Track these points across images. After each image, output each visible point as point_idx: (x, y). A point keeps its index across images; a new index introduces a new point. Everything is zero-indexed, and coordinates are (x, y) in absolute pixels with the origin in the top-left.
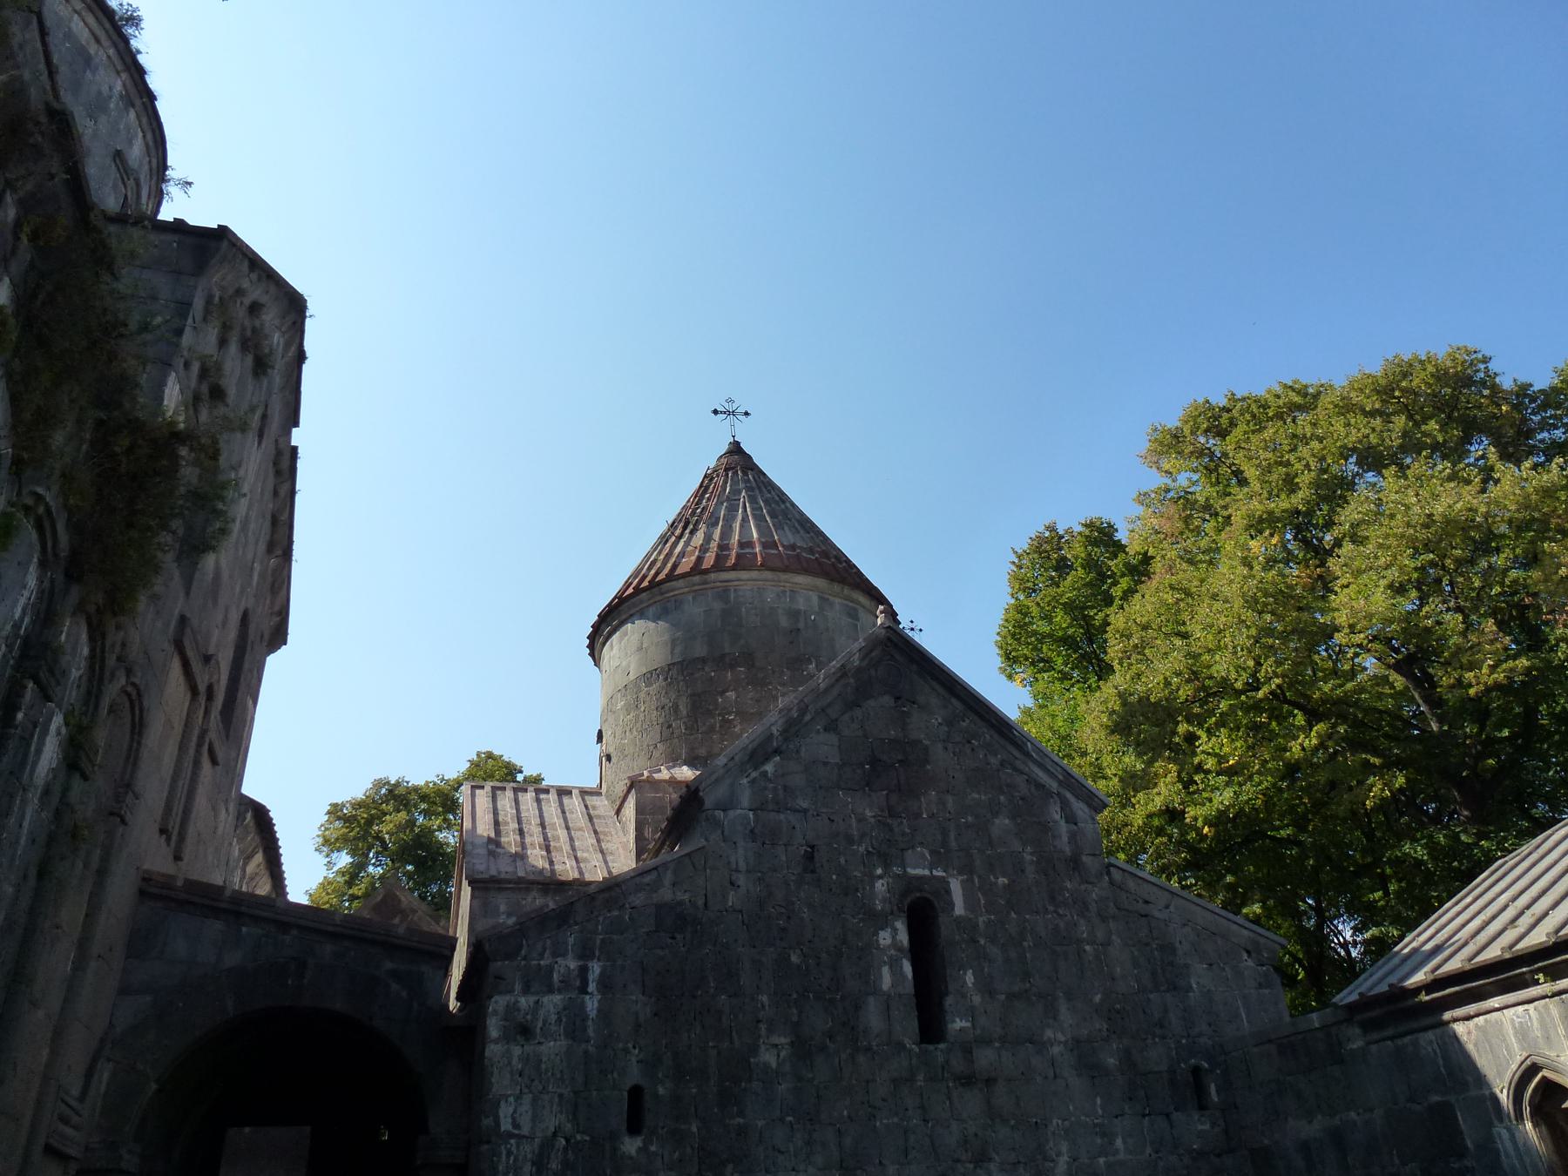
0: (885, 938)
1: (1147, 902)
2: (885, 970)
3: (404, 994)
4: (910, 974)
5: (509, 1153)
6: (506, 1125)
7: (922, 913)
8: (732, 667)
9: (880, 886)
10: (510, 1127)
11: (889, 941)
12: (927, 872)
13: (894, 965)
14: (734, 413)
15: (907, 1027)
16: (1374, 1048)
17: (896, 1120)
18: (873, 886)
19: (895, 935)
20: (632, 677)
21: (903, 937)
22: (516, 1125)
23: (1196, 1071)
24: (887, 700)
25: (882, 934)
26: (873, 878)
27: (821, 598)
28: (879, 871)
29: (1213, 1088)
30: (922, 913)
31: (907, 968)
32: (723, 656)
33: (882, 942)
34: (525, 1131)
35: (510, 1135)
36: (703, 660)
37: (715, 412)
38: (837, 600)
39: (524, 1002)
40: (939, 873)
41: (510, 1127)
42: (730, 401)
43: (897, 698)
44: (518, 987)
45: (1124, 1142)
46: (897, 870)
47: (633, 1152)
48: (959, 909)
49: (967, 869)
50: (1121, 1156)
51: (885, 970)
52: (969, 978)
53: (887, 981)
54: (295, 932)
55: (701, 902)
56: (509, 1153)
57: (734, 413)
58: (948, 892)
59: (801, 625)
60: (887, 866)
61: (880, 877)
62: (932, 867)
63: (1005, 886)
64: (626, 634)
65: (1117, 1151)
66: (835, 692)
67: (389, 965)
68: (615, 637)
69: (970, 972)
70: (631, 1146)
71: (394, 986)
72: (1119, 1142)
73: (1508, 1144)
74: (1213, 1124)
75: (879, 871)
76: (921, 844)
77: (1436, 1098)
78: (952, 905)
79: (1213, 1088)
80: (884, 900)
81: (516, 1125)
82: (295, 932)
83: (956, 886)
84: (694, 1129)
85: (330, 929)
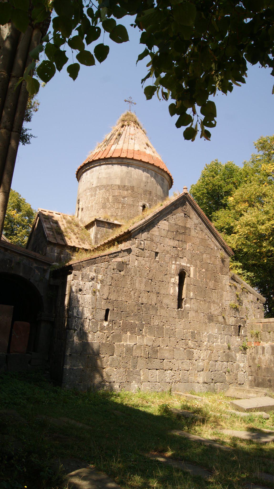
0: (173, 280)
2: (172, 288)
3: (39, 274)
4: (177, 291)
5: (76, 321)
6: (75, 314)
7: (182, 275)
8: (127, 190)
9: (173, 267)
10: (76, 315)
12: (185, 264)
13: (174, 288)
14: (131, 103)
15: (175, 304)
18: (172, 267)
19: (176, 279)
20: (94, 186)
21: (178, 281)
22: (78, 315)
24: (183, 214)
25: (172, 279)
27: (155, 173)
28: (174, 262)
29: (243, 331)
30: (182, 275)
32: (125, 186)
34: (80, 317)
35: (76, 317)
36: (119, 186)
37: (126, 101)
38: (159, 175)
39: (81, 283)
40: (188, 265)
41: (76, 315)
42: (131, 98)
43: (185, 214)
44: (80, 279)
45: (220, 341)
46: (177, 263)
48: (192, 276)
49: (196, 266)
50: (219, 344)
52: (192, 294)
53: (172, 291)
54: (9, 252)
56: (76, 321)
57: (131, 103)
59: (149, 181)
60: (176, 261)
62: (187, 263)
63: (204, 272)
64: (93, 172)
66: (169, 210)
67: (35, 265)
68: (88, 172)
69: (192, 293)
70: (105, 324)
71: (36, 271)
72: (219, 340)
74: (241, 340)
79: (243, 331)
81: (78, 315)
82: (9, 252)
83: (192, 269)
85: (19, 252)
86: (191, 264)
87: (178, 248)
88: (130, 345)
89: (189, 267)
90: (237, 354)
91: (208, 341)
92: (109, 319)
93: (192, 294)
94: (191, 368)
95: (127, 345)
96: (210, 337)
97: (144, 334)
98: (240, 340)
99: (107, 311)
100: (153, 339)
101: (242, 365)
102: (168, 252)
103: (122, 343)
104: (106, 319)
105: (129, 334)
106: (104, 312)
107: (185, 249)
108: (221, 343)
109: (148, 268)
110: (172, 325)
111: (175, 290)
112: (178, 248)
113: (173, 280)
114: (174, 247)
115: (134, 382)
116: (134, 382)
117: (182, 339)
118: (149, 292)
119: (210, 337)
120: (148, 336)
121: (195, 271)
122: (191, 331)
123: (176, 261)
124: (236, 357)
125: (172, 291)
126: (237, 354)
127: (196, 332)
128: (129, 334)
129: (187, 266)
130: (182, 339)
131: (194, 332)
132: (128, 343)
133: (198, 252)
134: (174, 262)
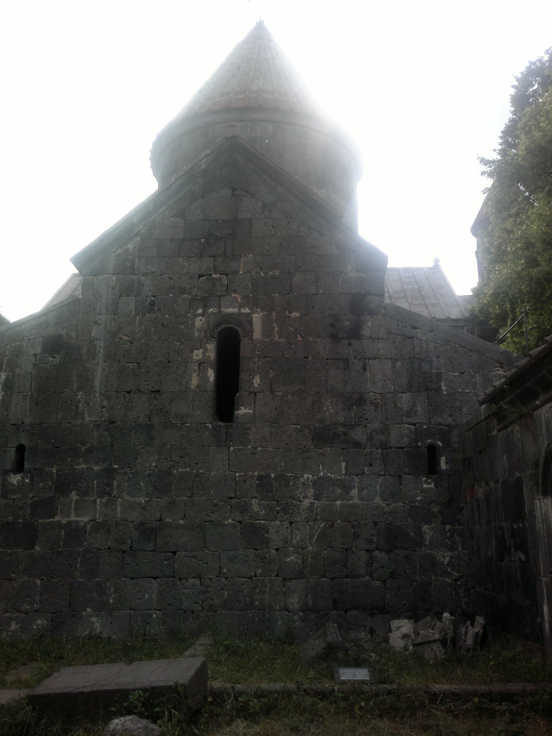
0: (198, 355)
1: (415, 328)
2: (194, 375)
9: (199, 322)
11: (201, 356)
12: (236, 310)
16: (500, 433)
17: (188, 470)
18: (194, 322)
23: (432, 449)
26: (196, 316)
31: (211, 375)
33: (195, 357)
40: (247, 310)
43: (234, 190)
45: (360, 492)
47: (15, 483)
48: (257, 334)
50: (356, 501)
51: (194, 375)
52: (257, 381)
53: (195, 382)
55: (74, 335)
58: (250, 323)
60: (205, 308)
61: (200, 315)
65: (352, 498)
70: (15, 479)
72: (354, 492)
73: (539, 513)
75: (200, 311)
76: (235, 291)
77: (518, 474)
78: (252, 331)
79: (443, 460)
80: (200, 330)
83: (257, 318)
84: (54, 470)
86: (254, 304)
87: (214, 276)
88: (77, 522)
89: (249, 314)
90: (425, 528)
91: (317, 497)
92: (27, 466)
93: (257, 381)
94: (259, 571)
95: (69, 523)
96: (319, 485)
97: (114, 493)
98: (432, 486)
99: (21, 449)
100: (140, 504)
101: (444, 557)
102: (182, 291)
103: (57, 519)
104: (19, 468)
105: (74, 496)
106: (12, 453)
107: (237, 272)
108: (361, 499)
109: (126, 338)
110: (199, 465)
111: (204, 378)
112: (214, 276)
113: (198, 355)
114: (200, 276)
115: (89, 610)
116: (89, 610)
117: (231, 498)
118: (129, 392)
119: (319, 485)
120: (126, 497)
121: (267, 322)
122: (256, 474)
123: (205, 308)
124: (420, 534)
125: (195, 382)
126: (425, 528)
127: (273, 475)
128: (74, 496)
129: (240, 314)
130: (231, 498)
131: (268, 476)
132: (73, 518)
133: (277, 272)
134: (200, 311)
